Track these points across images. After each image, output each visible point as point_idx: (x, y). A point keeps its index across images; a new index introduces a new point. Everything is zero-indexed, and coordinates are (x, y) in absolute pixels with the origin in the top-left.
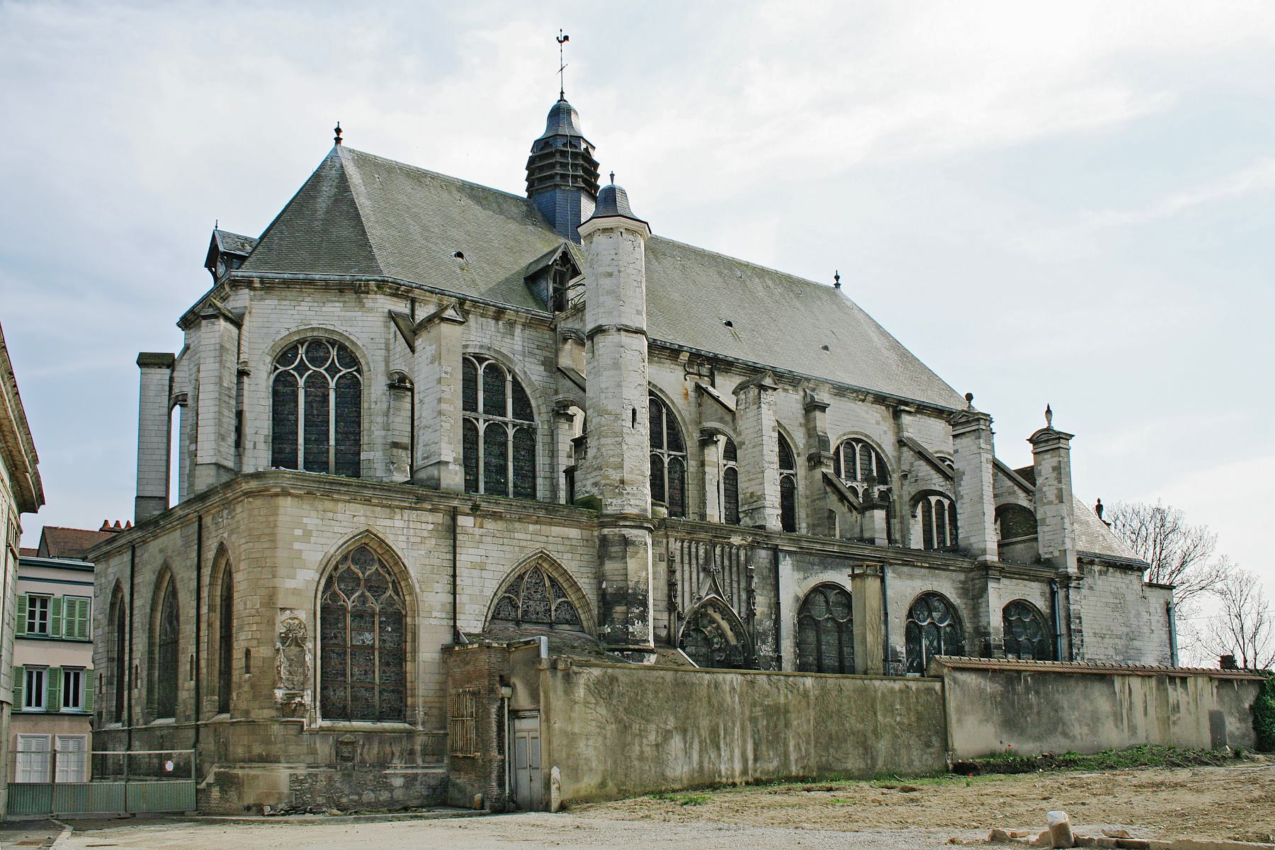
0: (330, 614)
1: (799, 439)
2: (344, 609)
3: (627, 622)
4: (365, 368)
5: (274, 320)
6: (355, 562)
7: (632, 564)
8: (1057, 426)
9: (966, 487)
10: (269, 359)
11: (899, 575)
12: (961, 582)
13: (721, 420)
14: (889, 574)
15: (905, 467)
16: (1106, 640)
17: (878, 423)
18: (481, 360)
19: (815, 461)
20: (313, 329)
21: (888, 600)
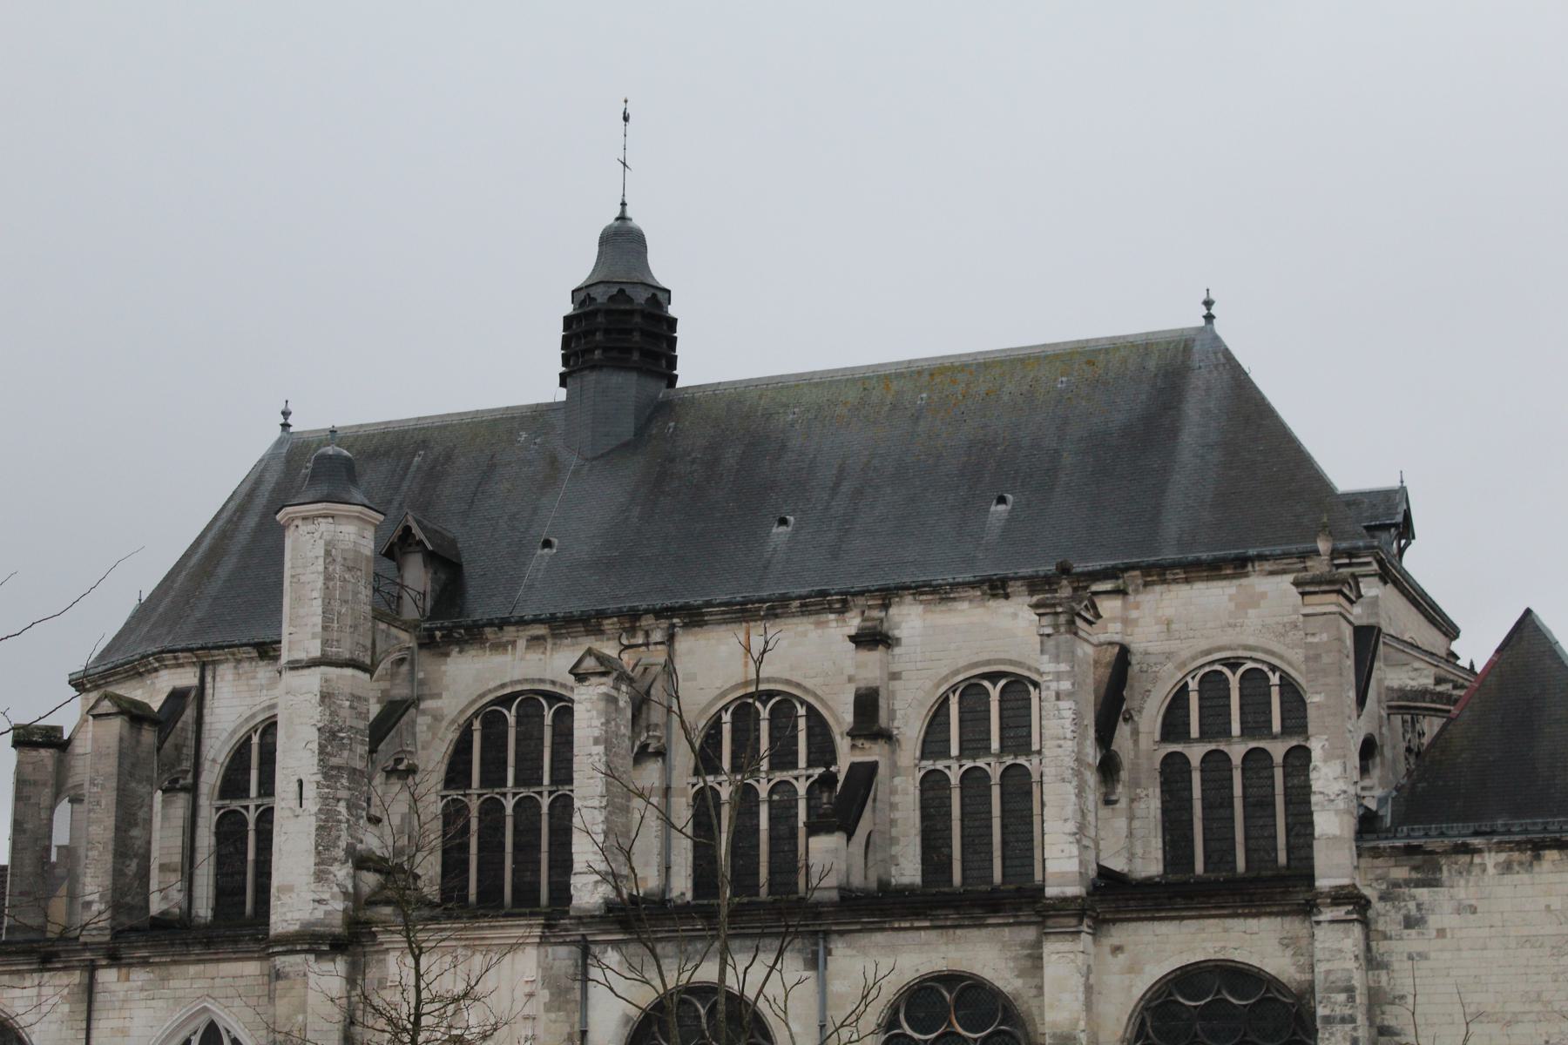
7: (282, 1007)
12: (1023, 945)
21: (830, 1002)
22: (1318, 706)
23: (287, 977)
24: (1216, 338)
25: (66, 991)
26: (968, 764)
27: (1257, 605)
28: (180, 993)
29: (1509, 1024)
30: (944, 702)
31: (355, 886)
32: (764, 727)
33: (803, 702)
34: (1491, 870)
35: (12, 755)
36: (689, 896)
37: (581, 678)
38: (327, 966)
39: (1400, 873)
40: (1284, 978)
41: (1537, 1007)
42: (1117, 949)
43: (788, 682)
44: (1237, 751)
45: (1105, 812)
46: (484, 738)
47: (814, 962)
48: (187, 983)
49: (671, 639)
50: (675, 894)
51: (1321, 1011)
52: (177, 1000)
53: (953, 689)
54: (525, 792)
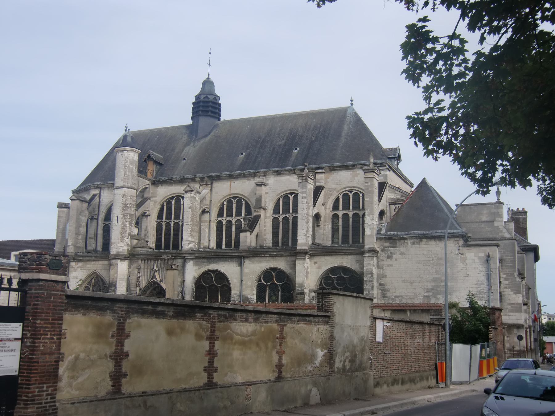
11: (253, 262)
22: (367, 201)
24: (353, 109)
26: (284, 216)
27: (357, 176)
29: (412, 283)
30: (279, 200)
31: (131, 243)
32: (234, 206)
33: (244, 200)
34: (409, 244)
35: (57, 210)
36: (215, 248)
37: (186, 192)
38: (123, 262)
39: (387, 244)
40: (356, 271)
41: (419, 279)
42: (315, 263)
43: (240, 194)
44: (351, 214)
46: (167, 207)
47: (240, 265)
50: (211, 247)
51: (365, 279)
53: (281, 197)
54: (176, 221)
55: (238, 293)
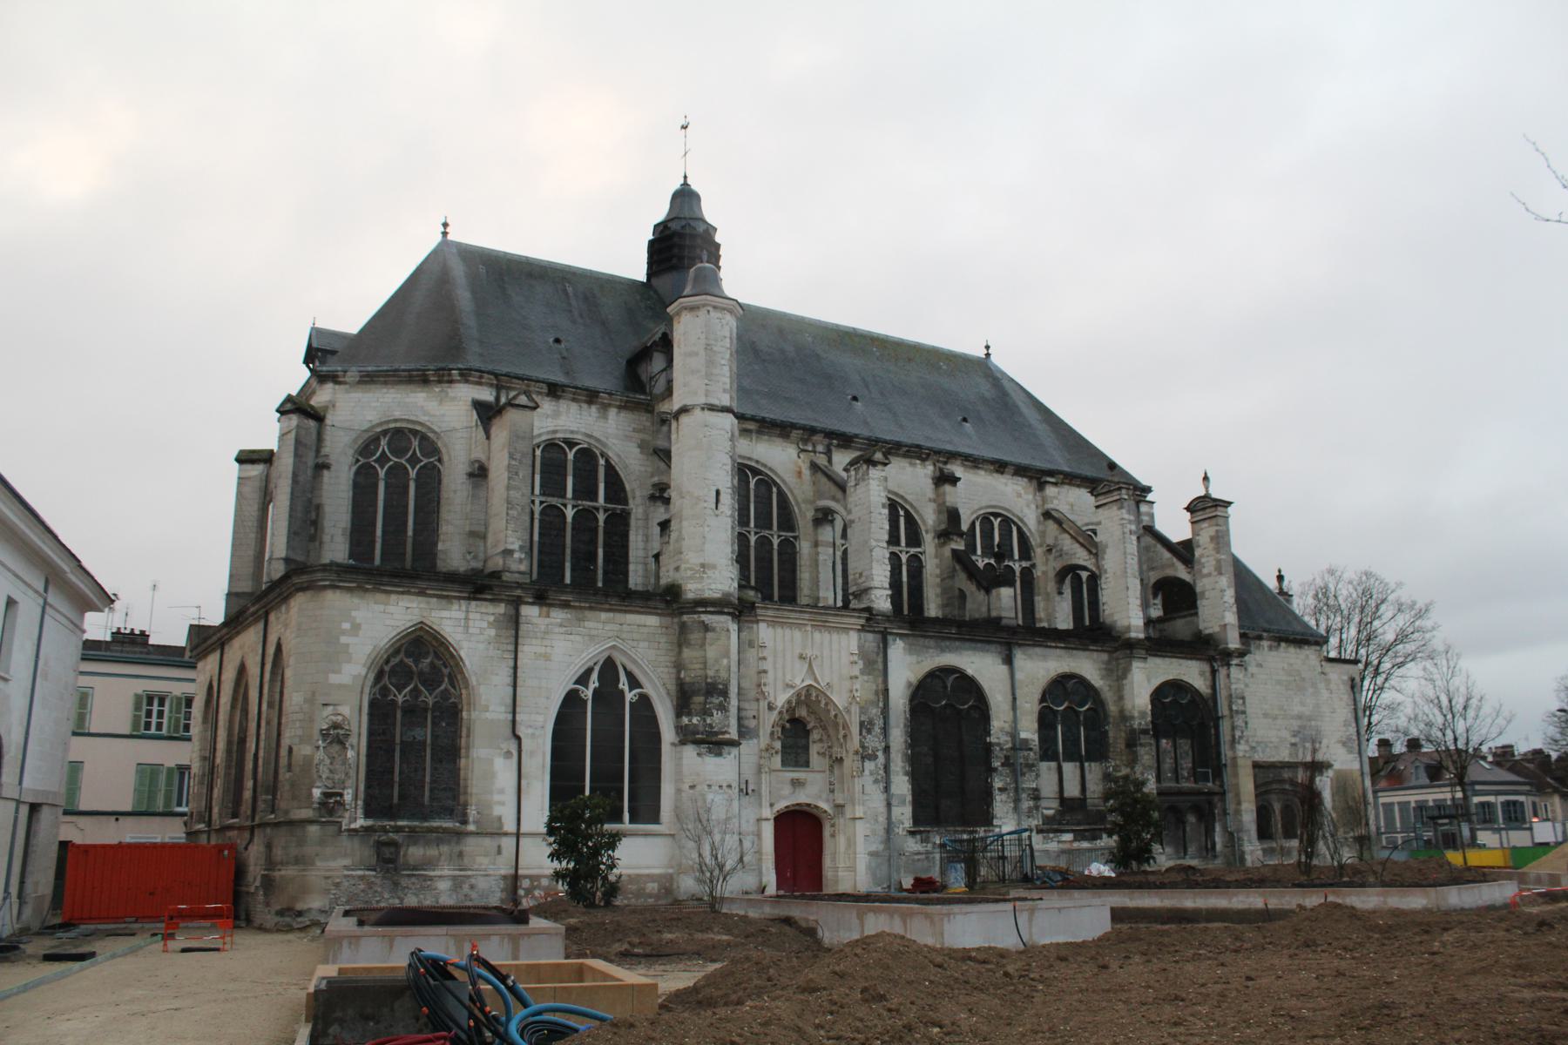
0: (380, 711)
1: (929, 518)
2: (394, 702)
3: (706, 712)
4: (445, 458)
5: (357, 410)
6: (408, 655)
7: (711, 652)
8: (1215, 493)
9: (1111, 562)
10: (351, 452)
11: (1030, 657)
13: (834, 498)
14: (1020, 658)
15: (1050, 541)
16: (1279, 722)
17: (1019, 495)
18: (571, 444)
19: (943, 536)
20: (396, 421)
23: (714, 630)
25: (492, 618)
28: (594, 632)
45: (1058, 598)
47: (1009, 661)
48: (600, 626)
49: (828, 453)
52: (592, 637)
55: (1007, 727)
